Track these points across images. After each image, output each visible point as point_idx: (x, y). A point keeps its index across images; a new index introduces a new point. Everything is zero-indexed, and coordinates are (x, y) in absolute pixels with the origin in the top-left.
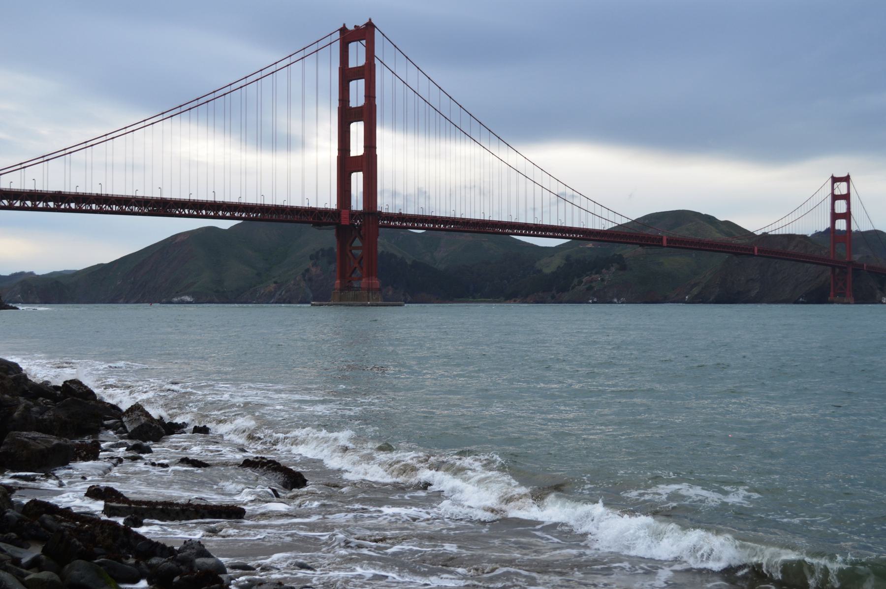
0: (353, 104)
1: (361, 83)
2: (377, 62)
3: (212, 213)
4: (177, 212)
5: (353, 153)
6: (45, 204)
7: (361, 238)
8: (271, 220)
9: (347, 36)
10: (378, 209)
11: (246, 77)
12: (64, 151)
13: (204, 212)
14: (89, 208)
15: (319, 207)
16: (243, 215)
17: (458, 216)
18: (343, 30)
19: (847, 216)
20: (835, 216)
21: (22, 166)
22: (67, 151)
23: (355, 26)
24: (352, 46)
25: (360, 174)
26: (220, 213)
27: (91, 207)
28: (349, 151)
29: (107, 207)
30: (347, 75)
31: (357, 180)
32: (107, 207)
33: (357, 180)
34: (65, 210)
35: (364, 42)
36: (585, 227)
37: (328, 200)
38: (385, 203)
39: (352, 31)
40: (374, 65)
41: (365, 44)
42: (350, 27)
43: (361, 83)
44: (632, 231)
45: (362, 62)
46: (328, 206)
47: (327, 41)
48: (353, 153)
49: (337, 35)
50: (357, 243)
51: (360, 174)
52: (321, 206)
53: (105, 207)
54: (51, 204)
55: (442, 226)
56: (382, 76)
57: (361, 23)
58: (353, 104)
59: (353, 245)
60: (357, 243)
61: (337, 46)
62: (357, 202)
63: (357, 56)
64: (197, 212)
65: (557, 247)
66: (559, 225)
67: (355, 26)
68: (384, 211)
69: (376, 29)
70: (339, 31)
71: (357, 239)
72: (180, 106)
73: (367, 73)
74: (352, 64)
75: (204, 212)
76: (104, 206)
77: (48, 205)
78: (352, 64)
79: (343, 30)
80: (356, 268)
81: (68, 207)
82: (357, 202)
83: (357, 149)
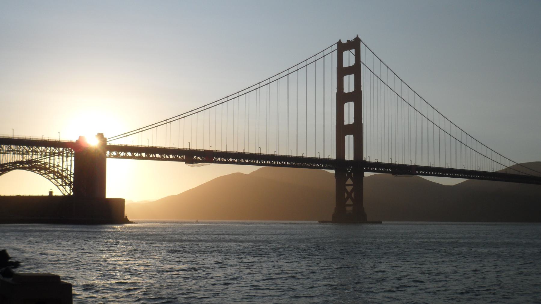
0: (346, 90)
1: (352, 77)
2: (361, 63)
3: (236, 161)
4: (225, 160)
5: (346, 122)
6: (139, 154)
7: (352, 179)
8: (276, 165)
9: (342, 47)
10: (363, 160)
11: (279, 74)
12: (166, 121)
13: (231, 160)
14: (168, 157)
15: (325, 157)
16: (257, 162)
17: (394, 162)
18: (339, 43)
21: (140, 130)
22: (168, 121)
23: (348, 41)
24: (346, 54)
25: (352, 137)
26: (242, 160)
27: (169, 157)
28: (344, 121)
29: (180, 157)
30: (342, 72)
31: (349, 140)
32: (180, 157)
33: (349, 140)
34: (152, 159)
35: (353, 51)
36: (465, 169)
37: (331, 154)
38: (368, 156)
39: (346, 43)
40: (361, 65)
41: (354, 53)
42: (344, 41)
43: (352, 77)
44: (525, 175)
45: (352, 63)
46: (330, 157)
47: (330, 50)
48: (346, 122)
49: (335, 47)
50: (349, 181)
51: (352, 137)
52: (326, 157)
53: (178, 157)
54: (144, 155)
55: (376, 169)
56: (364, 72)
57: (352, 38)
58: (346, 90)
59: (346, 183)
60: (349, 181)
61: (336, 53)
62: (349, 155)
63: (349, 59)
64: (226, 160)
65: (464, 182)
66: (447, 167)
67: (348, 41)
68: (367, 161)
69: (361, 42)
70: (336, 44)
71: (349, 178)
72: (238, 92)
73: (356, 70)
74: (345, 65)
75: (231, 160)
76: (178, 156)
77: (141, 155)
78: (345, 65)
79: (339, 43)
81: (154, 157)
82: (349, 155)
83: (349, 119)
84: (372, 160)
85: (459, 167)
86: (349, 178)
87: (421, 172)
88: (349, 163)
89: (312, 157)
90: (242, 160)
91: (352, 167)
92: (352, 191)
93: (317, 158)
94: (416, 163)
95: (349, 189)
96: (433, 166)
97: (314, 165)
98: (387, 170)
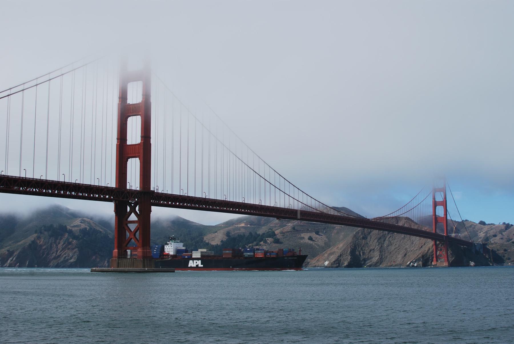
19: (444, 204)
20: (435, 204)
28: (126, 140)
37: (111, 182)
71: (133, 213)
80: (131, 239)
84: (160, 191)
85: (199, 195)
86: (133, 213)
87: (162, 202)
88: (133, 193)
89: (52, 181)
90: (73, 193)
91: (108, 196)
92: (136, 231)
93: (62, 182)
94: (164, 191)
95: (133, 227)
96: (186, 195)
97: (44, 191)
98: (162, 202)
